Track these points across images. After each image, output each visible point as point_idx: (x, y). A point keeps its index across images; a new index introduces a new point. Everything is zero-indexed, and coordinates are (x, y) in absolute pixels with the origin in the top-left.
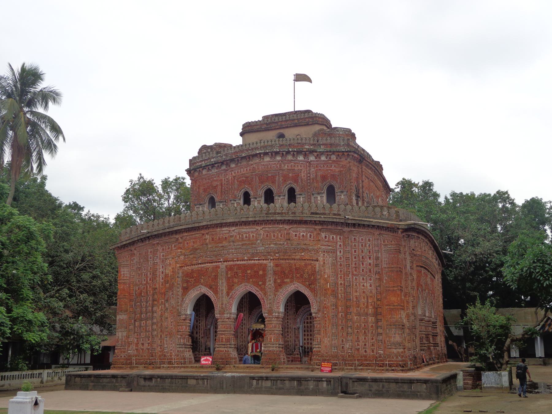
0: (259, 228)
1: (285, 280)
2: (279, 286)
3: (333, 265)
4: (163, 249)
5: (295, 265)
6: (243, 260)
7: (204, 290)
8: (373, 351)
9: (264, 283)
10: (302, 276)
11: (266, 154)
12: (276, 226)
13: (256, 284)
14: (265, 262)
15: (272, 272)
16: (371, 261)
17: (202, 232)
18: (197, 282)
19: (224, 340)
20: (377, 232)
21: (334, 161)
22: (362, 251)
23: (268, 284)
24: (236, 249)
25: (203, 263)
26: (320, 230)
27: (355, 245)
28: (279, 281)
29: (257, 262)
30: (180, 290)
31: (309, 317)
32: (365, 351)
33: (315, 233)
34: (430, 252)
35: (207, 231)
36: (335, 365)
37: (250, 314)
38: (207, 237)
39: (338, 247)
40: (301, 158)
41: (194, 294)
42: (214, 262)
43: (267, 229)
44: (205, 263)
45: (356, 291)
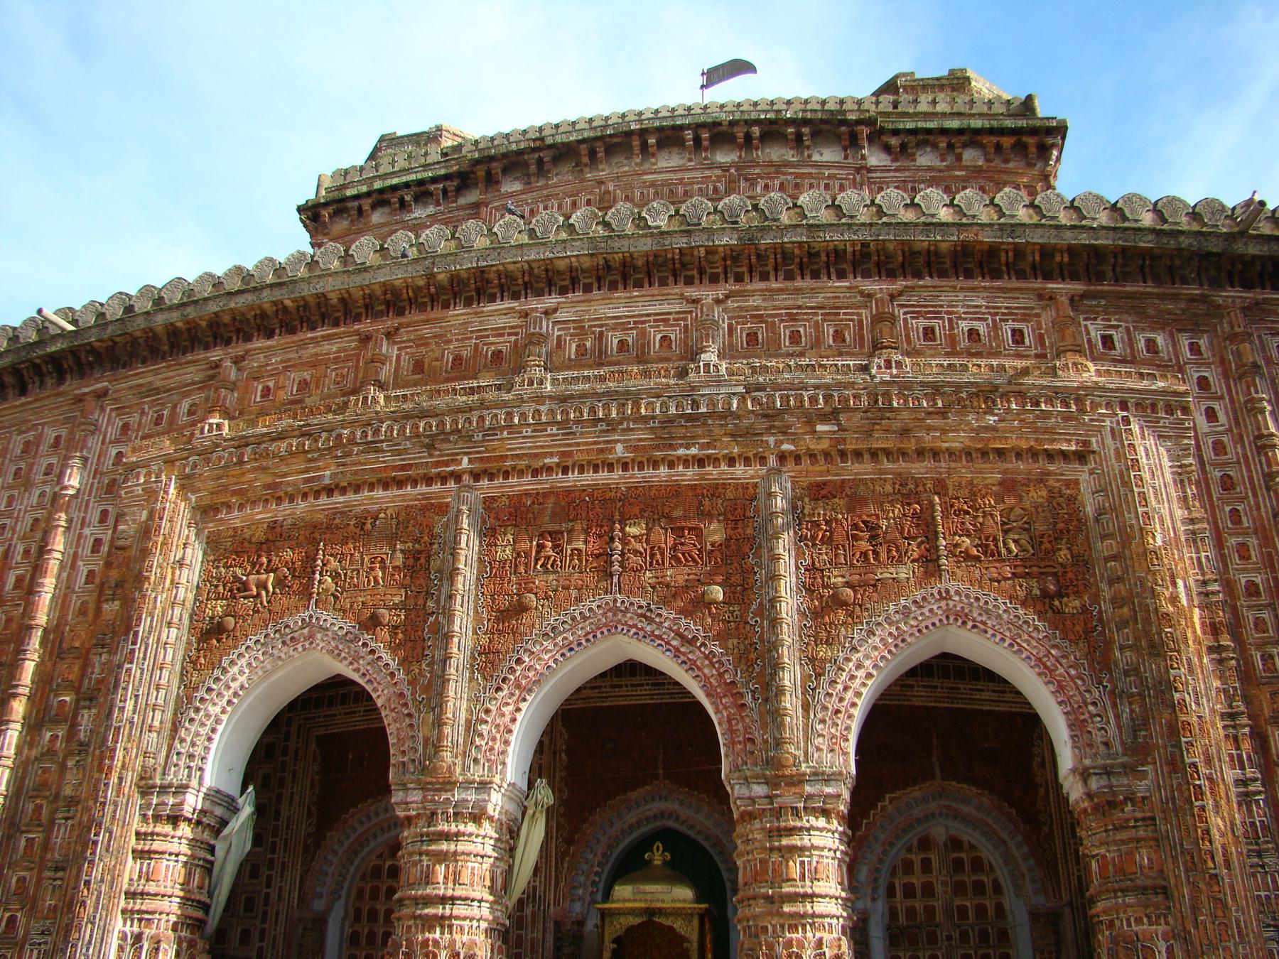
0: (707, 294)
4: (126, 428)
12: (807, 283)
14: (740, 470)
17: (365, 326)
21: (978, 171)
24: (563, 399)
29: (689, 475)
31: (916, 859)
33: (1046, 318)
35: (391, 322)
37: (569, 841)
42: (415, 483)
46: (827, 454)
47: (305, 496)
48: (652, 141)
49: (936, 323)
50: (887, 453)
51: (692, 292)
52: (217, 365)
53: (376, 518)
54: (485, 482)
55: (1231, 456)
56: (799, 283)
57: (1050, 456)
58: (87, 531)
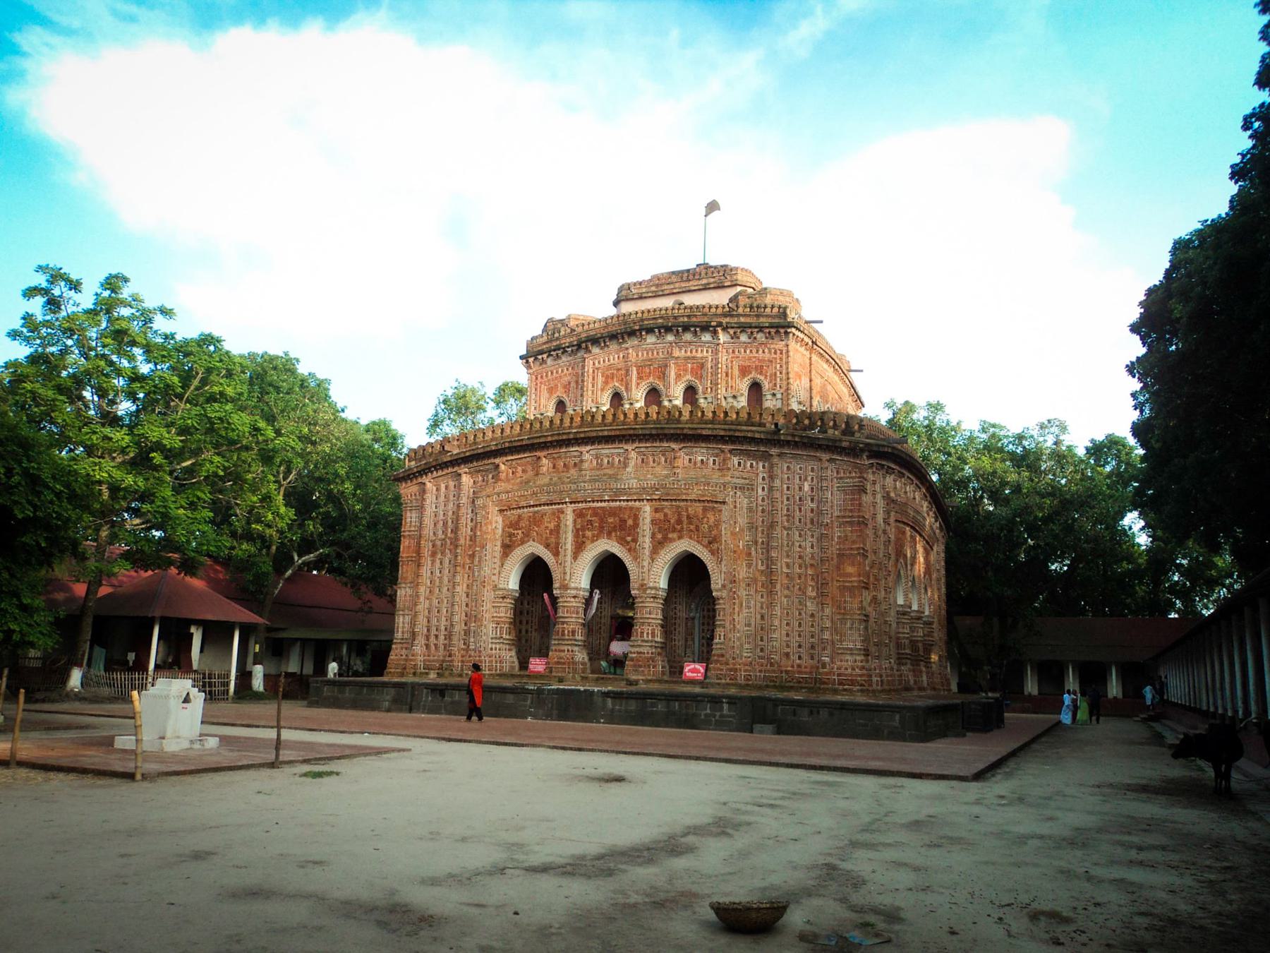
0: (629, 447)
1: (670, 536)
2: (658, 545)
3: (750, 510)
9: (635, 541)
11: (650, 331)
13: (622, 541)
15: (648, 520)
17: (538, 454)
20: (825, 456)
23: (640, 539)
26: (731, 451)
28: (659, 536)
30: (498, 548)
34: (925, 504)
35: (545, 453)
38: (544, 461)
39: (760, 480)
40: (707, 337)
41: (520, 555)
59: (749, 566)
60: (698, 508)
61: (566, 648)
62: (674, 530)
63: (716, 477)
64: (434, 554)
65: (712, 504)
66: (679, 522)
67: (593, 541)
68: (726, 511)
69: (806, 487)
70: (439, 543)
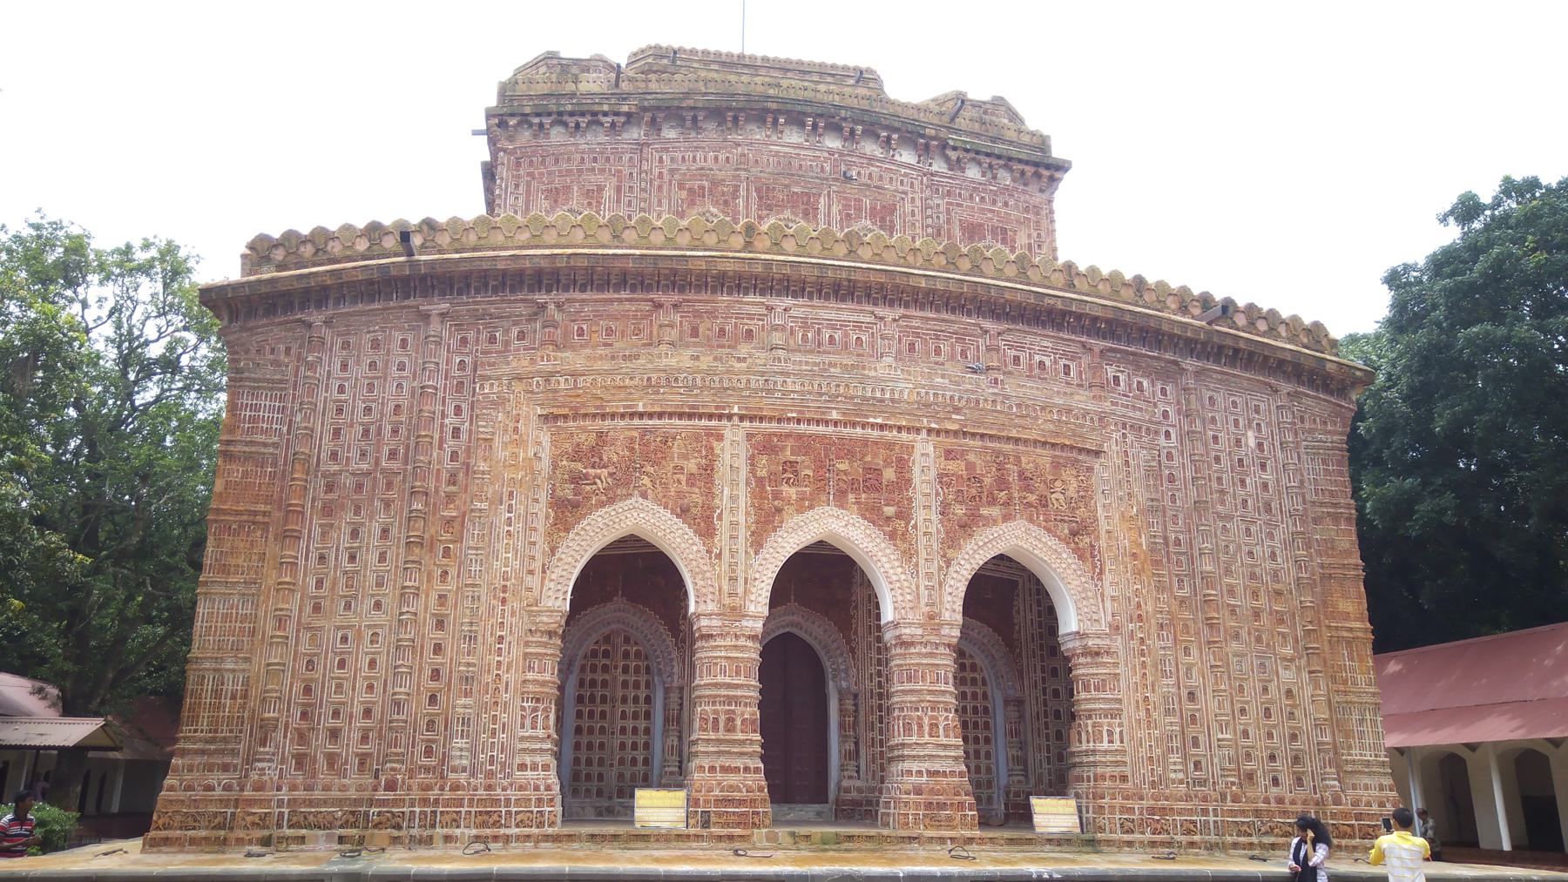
1: (984, 511)
2: (959, 530)
4: (464, 341)
5: (1018, 461)
6: (818, 422)
7: (645, 517)
8: (1299, 781)
9: (904, 515)
10: (1043, 502)
11: (797, 120)
12: (953, 317)
13: (872, 514)
14: (904, 435)
15: (933, 474)
16: (1268, 476)
18: (623, 484)
19: (739, 722)
20: (1286, 387)
22: (1238, 441)
23: (919, 515)
25: (651, 415)
27: (1213, 420)
28: (960, 510)
30: (542, 508)
32: (1275, 782)
35: (676, 297)
36: (1189, 832)
40: (907, 156)
42: (700, 416)
43: (915, 323)
44: (660, 415)
45: (1228, 572)
46: (955, 432)
47: (623, 416)
48: (782, 120)
49: (1022, 355)
50: (991, 437)
51: (880, 311)
52: (543, 307)
53: (674, 439)
54: (747, 424)
55: (1175, 463)
56: (944, 316)
57: (1081, 450)
58: (447, 421)
59: (1160, 588)
60: (1044, 457)
61: (739, 763)
62: (993, 501)
63: (1082, 400)
64: (328, 510)
65: (1078, 454)
66: (1002, 483)
67: (801, 510)
68: (1103, 472)
69: (1252, 442)
70: (348, 481)
